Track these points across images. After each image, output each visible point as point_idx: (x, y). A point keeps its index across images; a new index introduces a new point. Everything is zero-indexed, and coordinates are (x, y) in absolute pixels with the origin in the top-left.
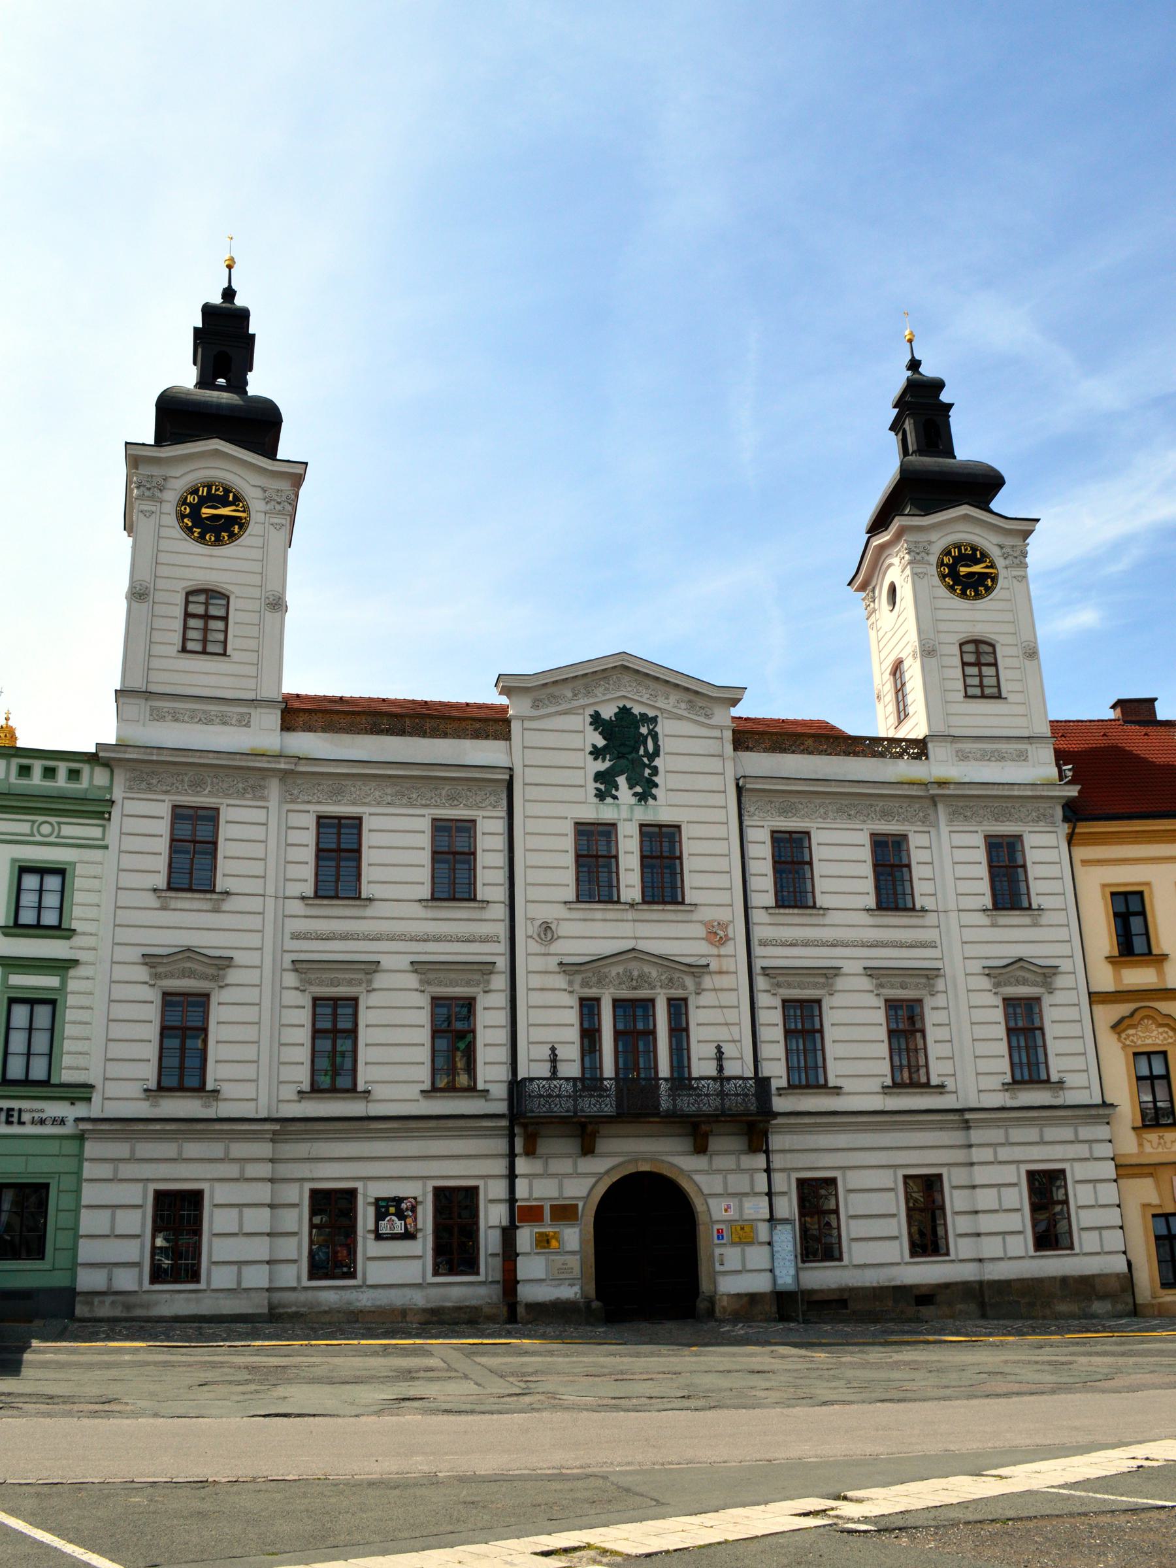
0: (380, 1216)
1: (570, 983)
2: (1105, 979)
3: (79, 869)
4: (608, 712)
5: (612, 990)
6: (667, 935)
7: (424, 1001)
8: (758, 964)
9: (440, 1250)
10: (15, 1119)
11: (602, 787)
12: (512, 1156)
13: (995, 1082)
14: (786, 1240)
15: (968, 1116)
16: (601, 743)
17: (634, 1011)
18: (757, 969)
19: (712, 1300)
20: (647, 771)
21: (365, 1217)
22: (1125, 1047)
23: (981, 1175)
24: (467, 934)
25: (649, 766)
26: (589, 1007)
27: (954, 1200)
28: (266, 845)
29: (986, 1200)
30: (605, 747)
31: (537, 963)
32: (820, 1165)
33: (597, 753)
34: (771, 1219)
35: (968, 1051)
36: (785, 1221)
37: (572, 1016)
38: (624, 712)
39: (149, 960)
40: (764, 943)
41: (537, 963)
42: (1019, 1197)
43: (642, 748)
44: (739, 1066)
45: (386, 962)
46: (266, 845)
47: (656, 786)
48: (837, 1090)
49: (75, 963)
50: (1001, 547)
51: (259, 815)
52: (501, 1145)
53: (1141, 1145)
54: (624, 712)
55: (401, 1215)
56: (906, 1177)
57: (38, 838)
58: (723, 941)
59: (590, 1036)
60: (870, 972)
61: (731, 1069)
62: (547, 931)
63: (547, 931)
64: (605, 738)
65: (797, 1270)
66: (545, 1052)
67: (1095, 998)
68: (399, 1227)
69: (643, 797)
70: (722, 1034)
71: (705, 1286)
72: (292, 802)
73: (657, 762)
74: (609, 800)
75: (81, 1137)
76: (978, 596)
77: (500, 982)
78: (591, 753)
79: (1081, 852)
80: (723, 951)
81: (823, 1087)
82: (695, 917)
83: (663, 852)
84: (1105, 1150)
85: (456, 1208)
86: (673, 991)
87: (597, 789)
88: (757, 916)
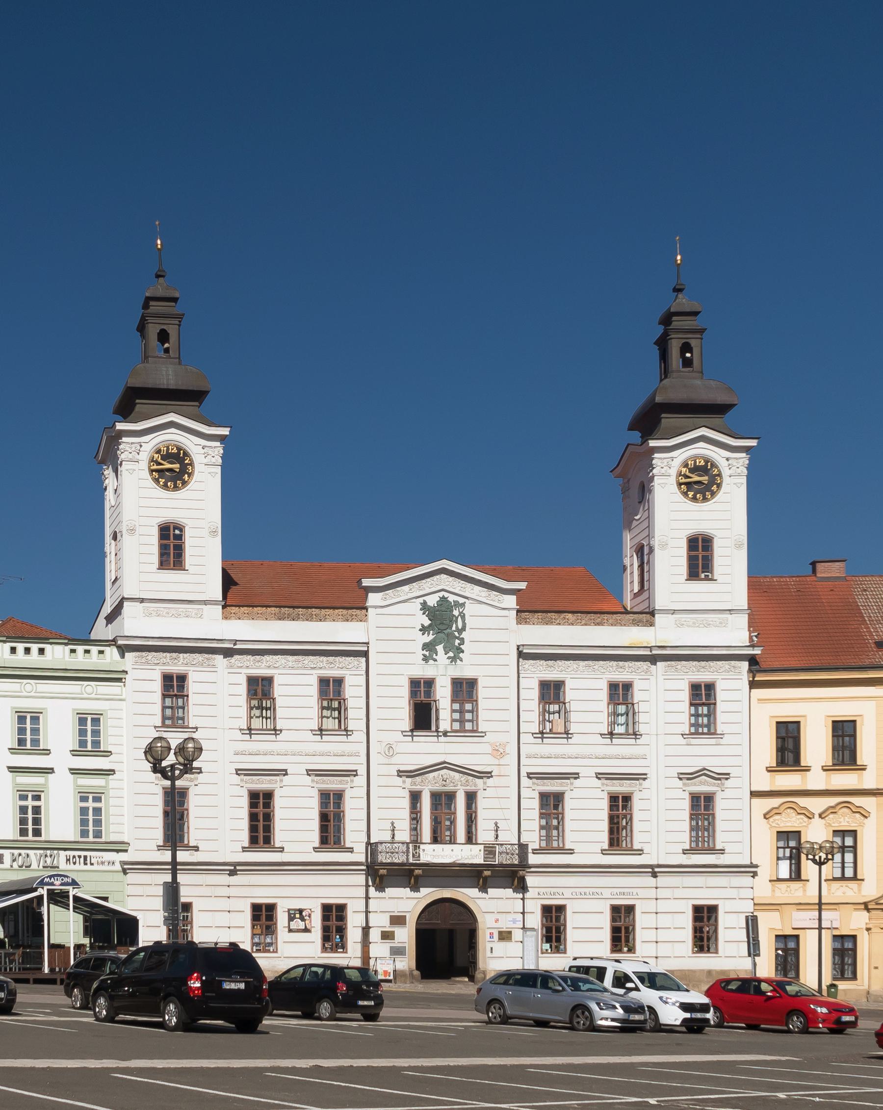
0: (291, 919)
1: (404, 782)
2: (764, 782)
3: (110, 714)
4: (432, 601)
7: (316, 794)
9: (326, 938)
11: (427, 653)
12: (367, 886)
13: (679, 848)
14: (534, 940)
15: (656, 870)
16: (427, 622)
18: (523, 773)
19: (484, 973)
20: (457, 642)
21: (282, 919)
22: (771, 827)
23: (662, 906)
25: (458, 638)
26: (415, 797)
28: (216, 694)
29: (664, 920)
30: (430, 625)
31: (385, 770)
33: (424, 629)
34: (524, 928)
35: (661, 827)
36: (533, 929)
37: (406, 803)
38: (443, 599)
41: (385, 770)
42: (687, 921)
44: (509, 836)
46: (216, 694)
47: (463, 652)
48: (571, 852)
49: (113, 771)
50: (727, 459)
52: (361, 879)
53: (773, 891)
54: (443, 599)
55: (302, 919)
57: (85, 696)
58: (502, 755)
59: (415, 817)
61: (503, 837)
65: (538, 957)
66: (388, 826)
67: (754, 794)
68: (301, 925)
69: (453, 659)
70: (497, 815)
71: (481, 965)
72: (231, 667)
74: (431, 662)
75: (125, 872)
76: (705, 499)
77: (361, 780)
78: (420, 630)
79: (758, 693)
80: (502, 762)
81: (562, 850)
84: (748, 893)
85: (334, 917)
88: (525, 738)
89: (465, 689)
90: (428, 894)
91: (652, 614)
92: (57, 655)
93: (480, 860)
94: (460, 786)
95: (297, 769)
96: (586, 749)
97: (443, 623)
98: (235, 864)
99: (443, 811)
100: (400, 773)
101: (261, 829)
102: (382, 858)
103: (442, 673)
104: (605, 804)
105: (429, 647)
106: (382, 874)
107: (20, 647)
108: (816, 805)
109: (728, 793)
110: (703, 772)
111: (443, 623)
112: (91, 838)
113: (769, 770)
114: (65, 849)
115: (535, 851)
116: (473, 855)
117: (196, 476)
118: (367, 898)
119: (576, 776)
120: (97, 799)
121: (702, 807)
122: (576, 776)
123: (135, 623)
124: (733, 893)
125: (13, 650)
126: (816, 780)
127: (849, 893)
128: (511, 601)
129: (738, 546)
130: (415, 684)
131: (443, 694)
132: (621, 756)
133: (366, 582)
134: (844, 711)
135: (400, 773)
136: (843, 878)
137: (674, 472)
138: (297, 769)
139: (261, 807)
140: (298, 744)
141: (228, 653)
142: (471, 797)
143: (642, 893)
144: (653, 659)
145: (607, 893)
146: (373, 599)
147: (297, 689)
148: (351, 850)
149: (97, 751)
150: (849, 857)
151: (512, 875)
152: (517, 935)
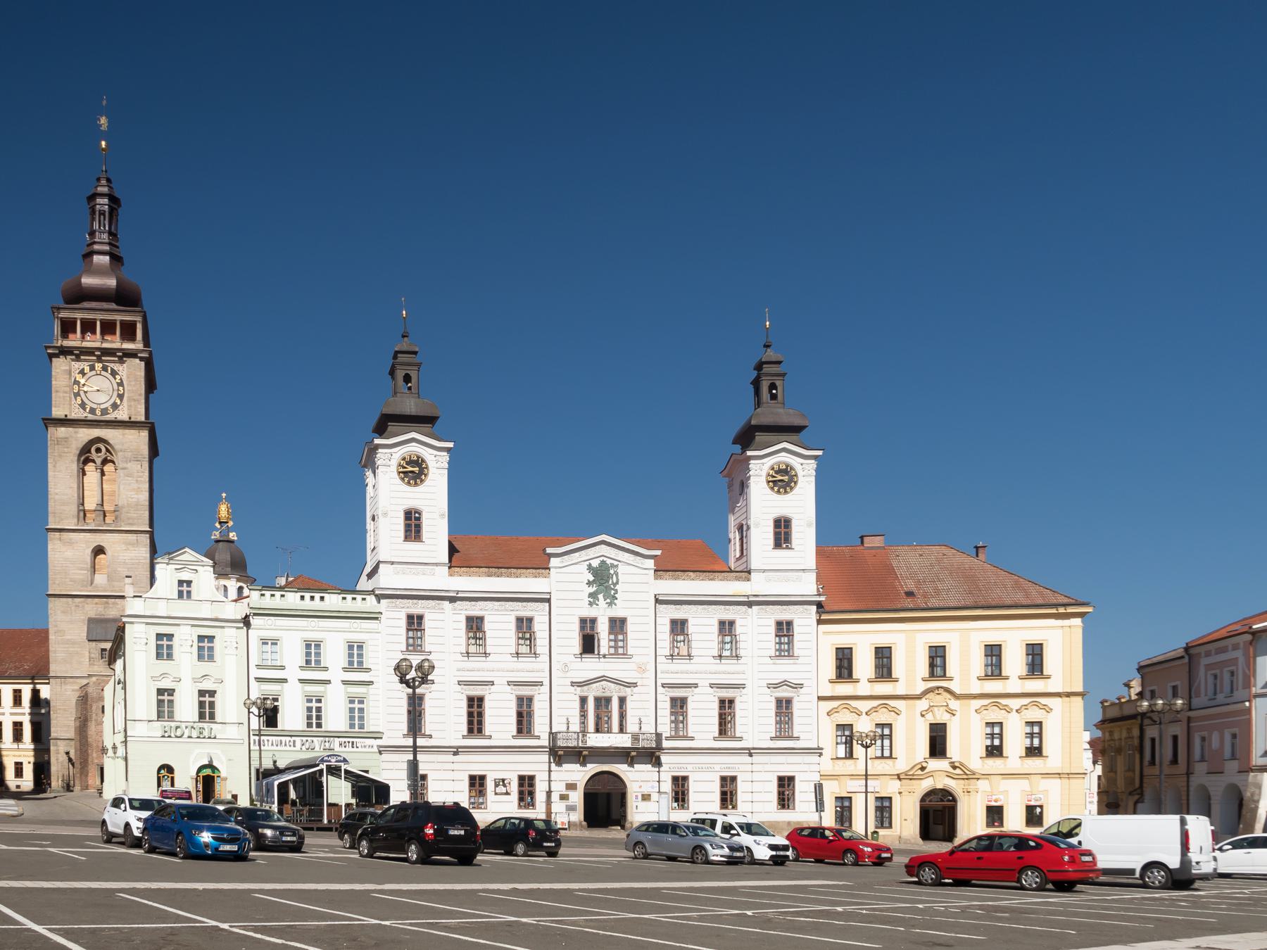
0: (497, 785)
2: (828, 690)
4: (595, 563)
9: (521, 799)
16: (592, 578)
18: (659, 684)
21: (490, 785)
23: (756, 776)
24: (531, 669)
26: (583, 700)
27: (741, 787)
28: (445, 627)
29: (757, 787)
33: (589, 583)
35: (755, 721)
37: (577, 704)
38: (603, 562)
42: (773, 787)
44: (649, 728)
46: (445, 627)
48: (692, 739)
51: (441, 616)
52: (545, 757)
54: (603, 562)
55: (504, 785)
59: (584, 715)
60: (712, 686)
67: (820, 698)
69: (610, 604)
70: (640, 713)
71: (629, 817)
75: (380, 752)
76: (786, 492)
77: (546, 688)
79: (823, 627)
84: (816, 768)
85: (527, 784)
89: (618, 625)
90: (593, 768)
91: (749, 572)
92: (333, 601)
93: (629, 745)
94: (614, 692)
95: (501, 680)
96: (703, 668)
97: (602, 578)
98: (458, 747)
99: (602, 710)
100: (573, 684)
101: (475, 722)
102: (560, 743)
103: (602, 614)
104: (716, 705)
105: (593, 595)
106: (560, 754)
107: (307, 596)
108: (864, 706)
109: (802, 698)
110: (784, 683)
111: (602, 578)
112: (357, 729)
113: (831, 682)
115: (667, 739)
116: (624, 741)
117: (430, 476)
118: (550, 771)
119: (696, 686)
120: (361, 702)
121: (784, 707)
122: (696, 686)
123: (387, 579)
124: (805, 768)
125: (302, 598)
126: (863, 688)
127: (887, 767)
128: (650, 563)
129: (809, 525)
130: (583, 621)
131: (603, 629)
132: (728, 671)
133: (549, 550)
134: (883, 641)
135: (573, 684)
136: (882, 757)
137: (764, 473)
138: (501, 680)
139: (475, 708)
140: (502, 666)
141: (452, 600)
142: (622, 701)
143: (742, 768)
144: (750, 604)
145: (717, 768)
146: (554, 562)
147: (500, 624)
148: (538, 737)
149: (361, 668)
150: (887, 742)
151: (651, 756)
152: (655, 797)
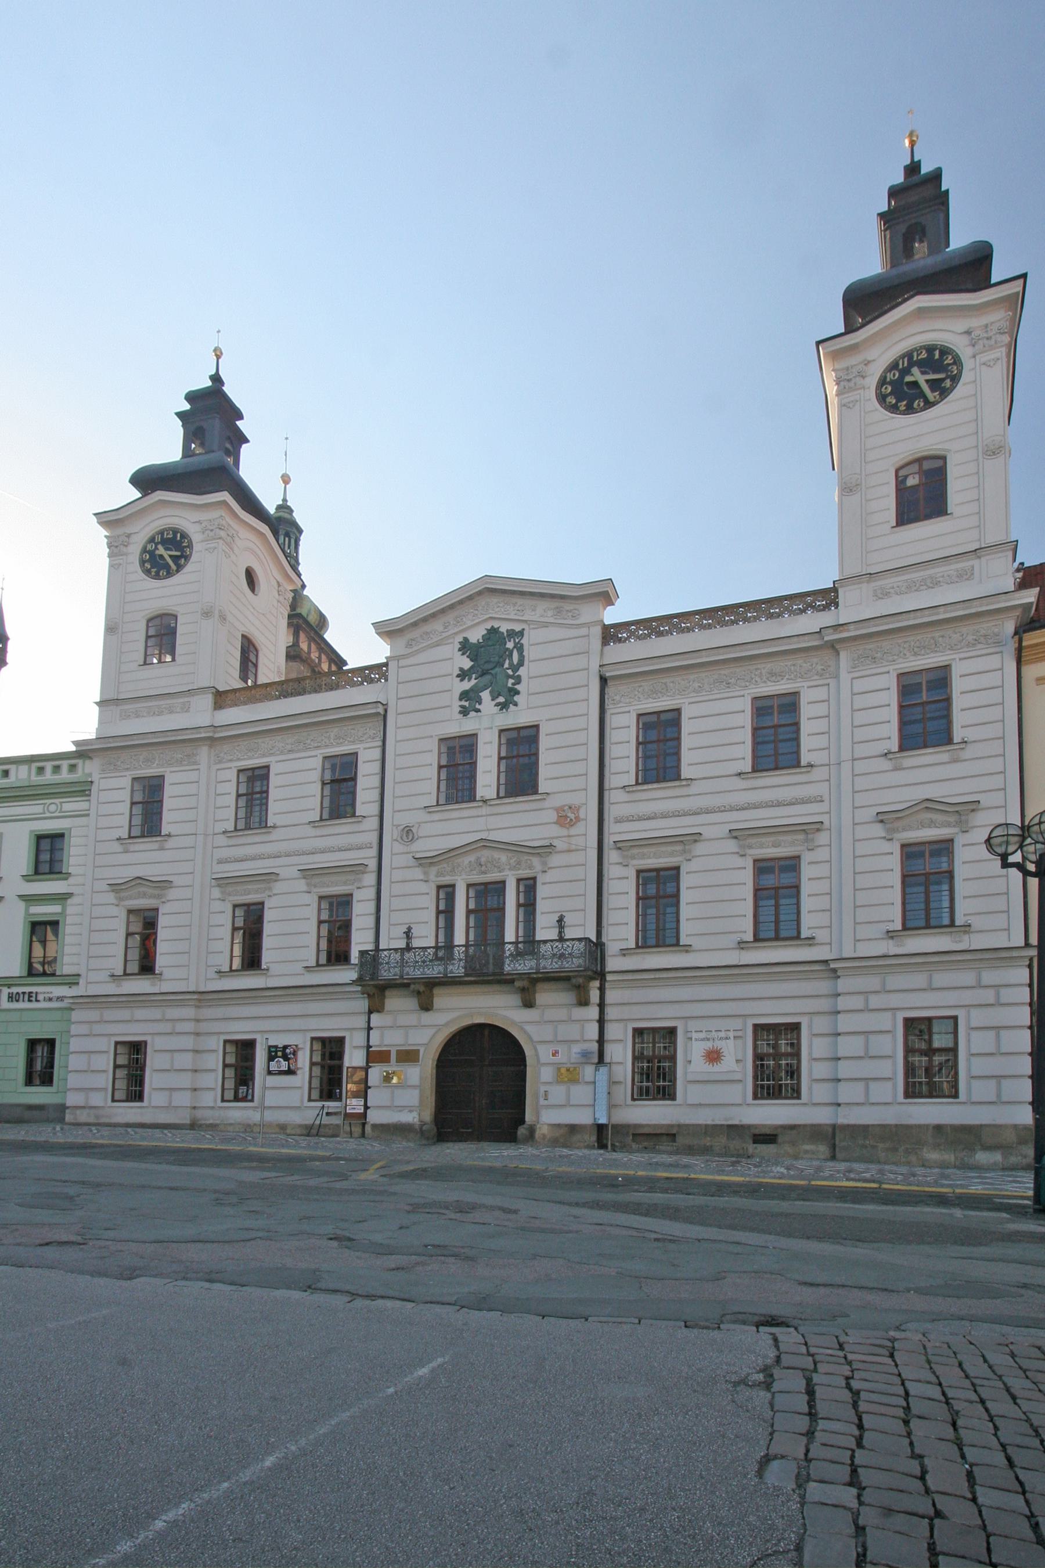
1: (425, 873)
5: (464, 877)
6: (520, 823)
8: (609, 840)
10: (33, 999)
11: (466, 704)
16: (467, 664)
17: (488, 897)
30: (472, 667)
32: (659, 1018)
33: (463, 675)
39: (116, 888)
40: (619, 821)
43: (507, 662)
45: (283, 873)
47: (518, 693)
48: (687, 949)
56: (756, 1027)
58: (572, 824)
60: (734, 834)
62: (408, 834)
63: (408, 834)
64: (472, 660)
69: (504, 706)
73: (522, 672)
77: (370, 879)
78: (458, 676)
80: (573, 831)
82: (547, 804)
83: (522, 750)
86: (520, 872)
87: (461, 706)
88: (613, 796)
114: (9, 986)
115: (624, 952)
